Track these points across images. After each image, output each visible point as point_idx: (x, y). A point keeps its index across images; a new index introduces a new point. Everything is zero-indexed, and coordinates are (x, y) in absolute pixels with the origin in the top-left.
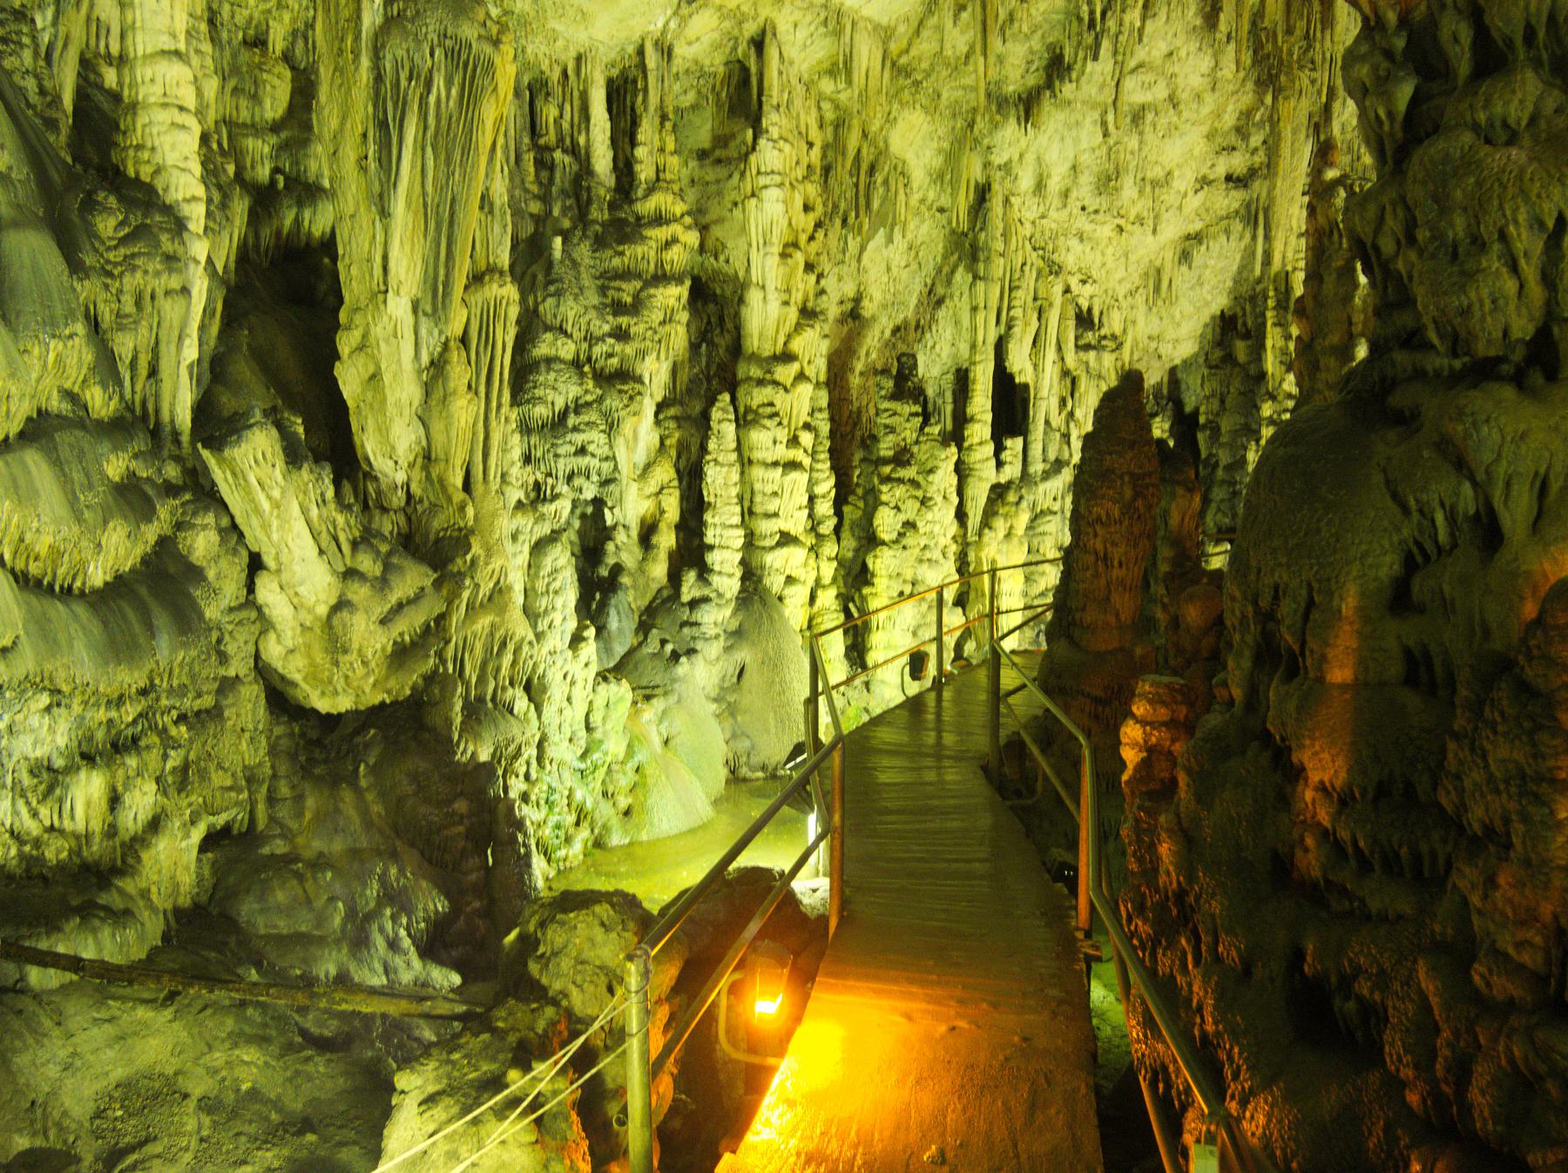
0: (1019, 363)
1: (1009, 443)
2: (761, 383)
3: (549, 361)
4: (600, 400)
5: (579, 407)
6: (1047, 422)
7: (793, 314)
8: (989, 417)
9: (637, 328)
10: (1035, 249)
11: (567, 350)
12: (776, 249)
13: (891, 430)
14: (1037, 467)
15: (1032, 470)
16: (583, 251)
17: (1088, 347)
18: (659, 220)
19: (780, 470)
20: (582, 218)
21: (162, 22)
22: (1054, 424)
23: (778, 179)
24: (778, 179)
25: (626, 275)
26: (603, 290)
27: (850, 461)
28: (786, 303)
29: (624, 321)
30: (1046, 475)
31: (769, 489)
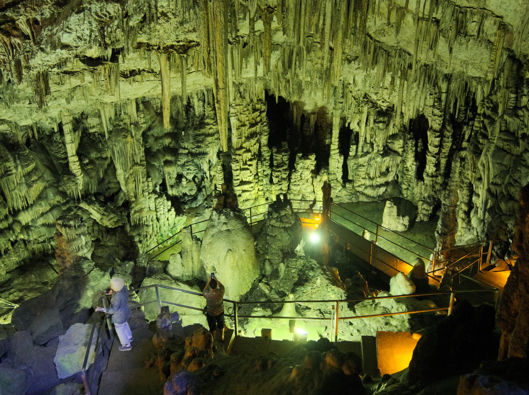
0: (354, 126)
1: (351, 146)
2: (233, 155)
3: (181, 154)
4: (193, 160)
5: (187, 162)
6: (365, 141)
7: (244, 139)
8: (337, 143)
9: (203, 145)
10: (355, 99)
11: (187, 151)
12: (235, 128)
13: (276, 160)
14: (360, 153)
15: (358, 154)
16: (191, 132)
17: (380, 122)
18: (208, 124)
19: (238, 172)
20: (193, 125)
21: (71, 152)
22: (368, 141)
23: (234, 115)
24: (234, 115)
25: (200, 135)
26: (195, 139)
27: (325, 137)
28: (241, 138)
29: (199, 144)
30: (362, 156)
31: (236, 175)
